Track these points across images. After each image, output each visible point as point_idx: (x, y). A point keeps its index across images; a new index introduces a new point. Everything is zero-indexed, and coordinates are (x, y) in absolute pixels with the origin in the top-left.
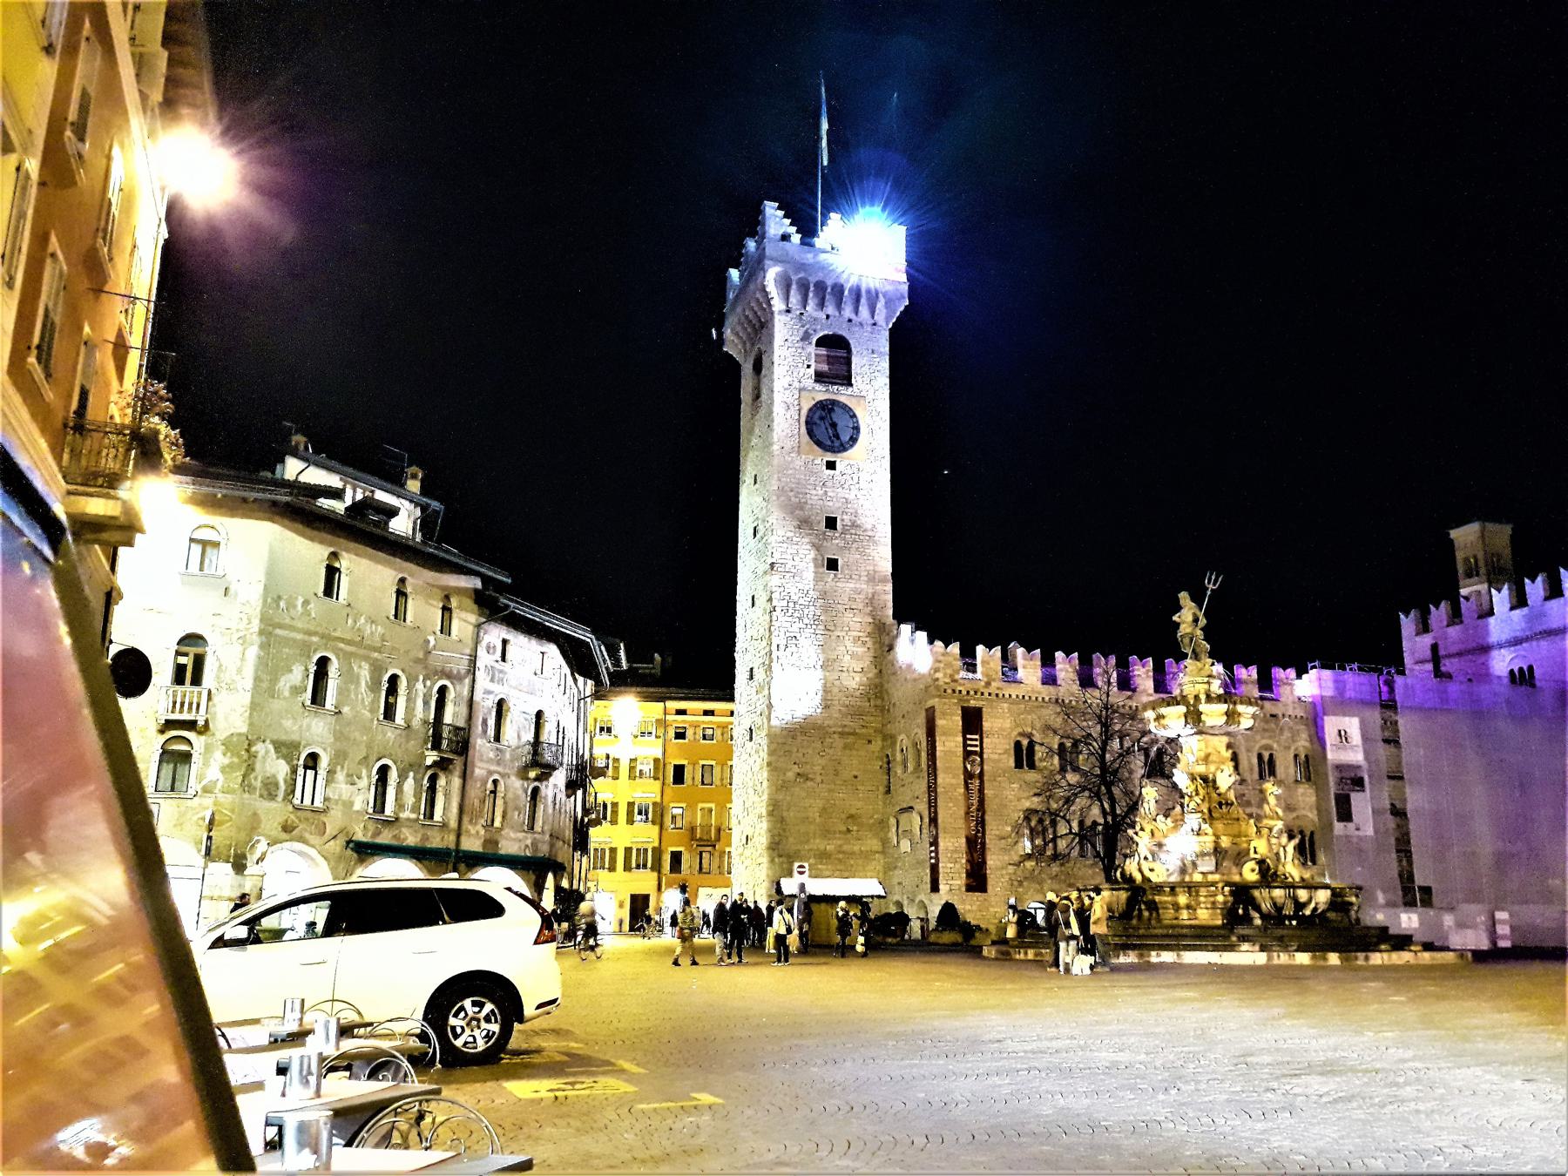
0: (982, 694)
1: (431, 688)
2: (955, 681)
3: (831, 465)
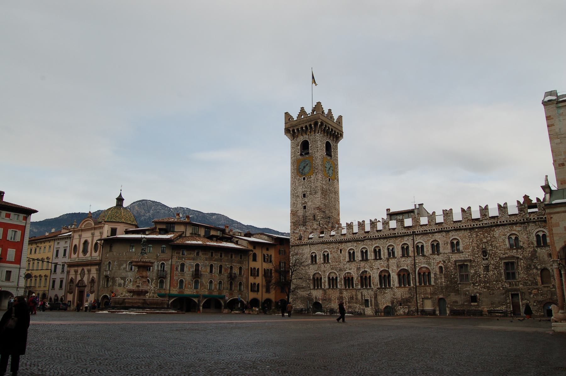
0: (302, 243)
1: (159, 263)
2: (295, 240)
3: (304, 179)
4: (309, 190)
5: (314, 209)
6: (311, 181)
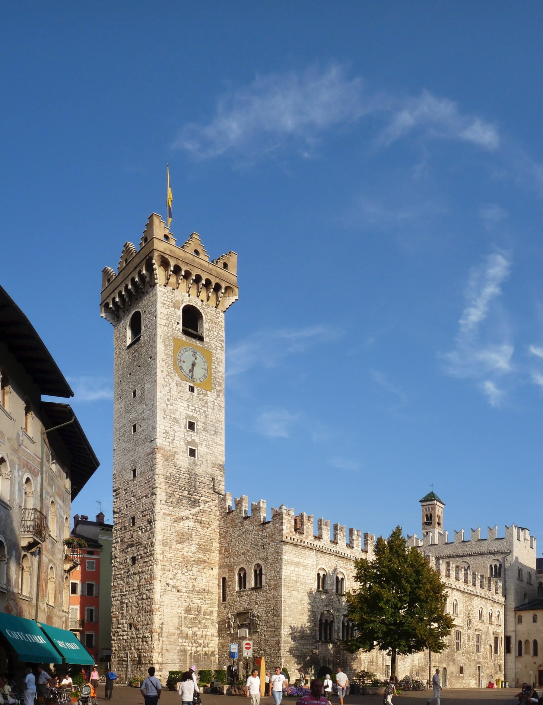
2: (291, 532)
3: (192, 389)
4: (204, 421)
5: (214, 465)
6: (206, 403)
